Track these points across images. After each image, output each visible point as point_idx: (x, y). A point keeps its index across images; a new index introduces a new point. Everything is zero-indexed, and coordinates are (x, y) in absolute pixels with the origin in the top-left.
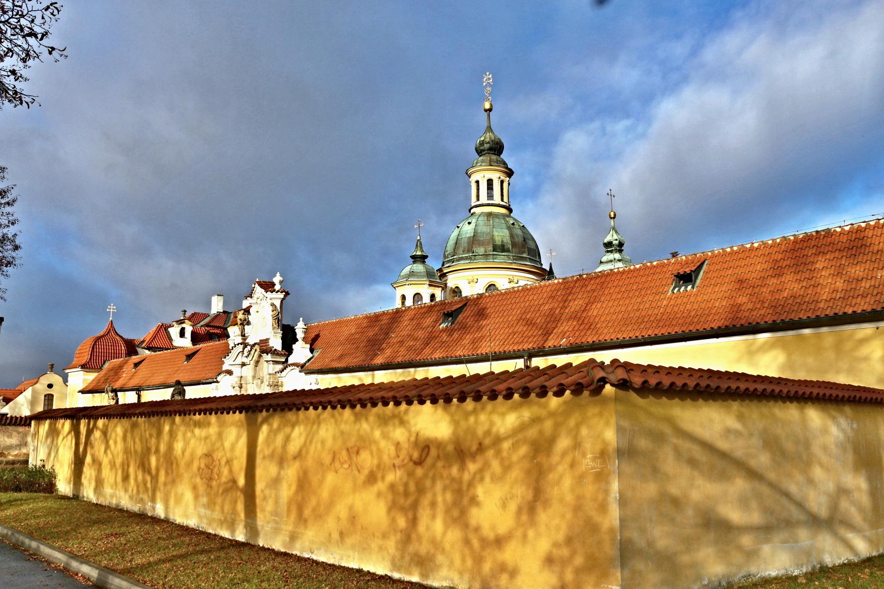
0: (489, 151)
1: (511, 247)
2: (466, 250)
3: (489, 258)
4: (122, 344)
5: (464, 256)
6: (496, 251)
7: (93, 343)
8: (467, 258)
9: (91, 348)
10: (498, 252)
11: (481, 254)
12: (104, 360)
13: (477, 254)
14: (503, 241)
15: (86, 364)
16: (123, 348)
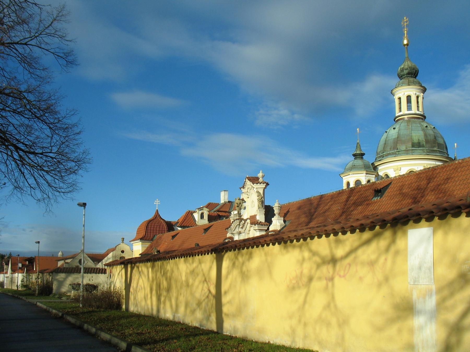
0: (407, 75)
1: (425, 143)
2: (392, 148)
3: (409, 152)
4: (164, 225)
5: (391, 152)
6: (414, 147)
7: (147, 224)
8: (393, 154)
9: (146, 228)
10: (416, 148)
11: (403, 150)
12: (154, 235)
13: (400, 150)
14: (419, 140)
15: (143, 238)
16: (165, 226)
